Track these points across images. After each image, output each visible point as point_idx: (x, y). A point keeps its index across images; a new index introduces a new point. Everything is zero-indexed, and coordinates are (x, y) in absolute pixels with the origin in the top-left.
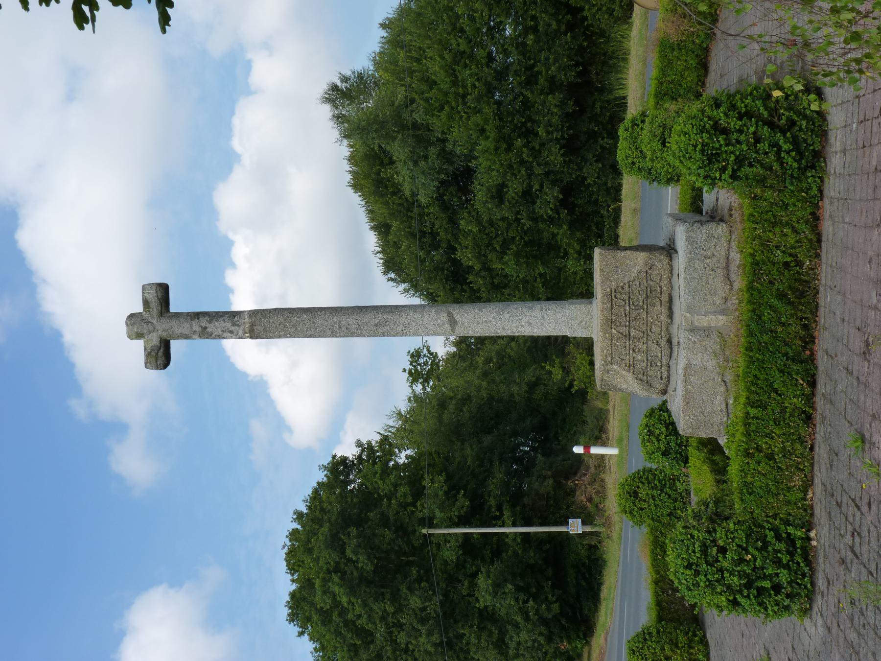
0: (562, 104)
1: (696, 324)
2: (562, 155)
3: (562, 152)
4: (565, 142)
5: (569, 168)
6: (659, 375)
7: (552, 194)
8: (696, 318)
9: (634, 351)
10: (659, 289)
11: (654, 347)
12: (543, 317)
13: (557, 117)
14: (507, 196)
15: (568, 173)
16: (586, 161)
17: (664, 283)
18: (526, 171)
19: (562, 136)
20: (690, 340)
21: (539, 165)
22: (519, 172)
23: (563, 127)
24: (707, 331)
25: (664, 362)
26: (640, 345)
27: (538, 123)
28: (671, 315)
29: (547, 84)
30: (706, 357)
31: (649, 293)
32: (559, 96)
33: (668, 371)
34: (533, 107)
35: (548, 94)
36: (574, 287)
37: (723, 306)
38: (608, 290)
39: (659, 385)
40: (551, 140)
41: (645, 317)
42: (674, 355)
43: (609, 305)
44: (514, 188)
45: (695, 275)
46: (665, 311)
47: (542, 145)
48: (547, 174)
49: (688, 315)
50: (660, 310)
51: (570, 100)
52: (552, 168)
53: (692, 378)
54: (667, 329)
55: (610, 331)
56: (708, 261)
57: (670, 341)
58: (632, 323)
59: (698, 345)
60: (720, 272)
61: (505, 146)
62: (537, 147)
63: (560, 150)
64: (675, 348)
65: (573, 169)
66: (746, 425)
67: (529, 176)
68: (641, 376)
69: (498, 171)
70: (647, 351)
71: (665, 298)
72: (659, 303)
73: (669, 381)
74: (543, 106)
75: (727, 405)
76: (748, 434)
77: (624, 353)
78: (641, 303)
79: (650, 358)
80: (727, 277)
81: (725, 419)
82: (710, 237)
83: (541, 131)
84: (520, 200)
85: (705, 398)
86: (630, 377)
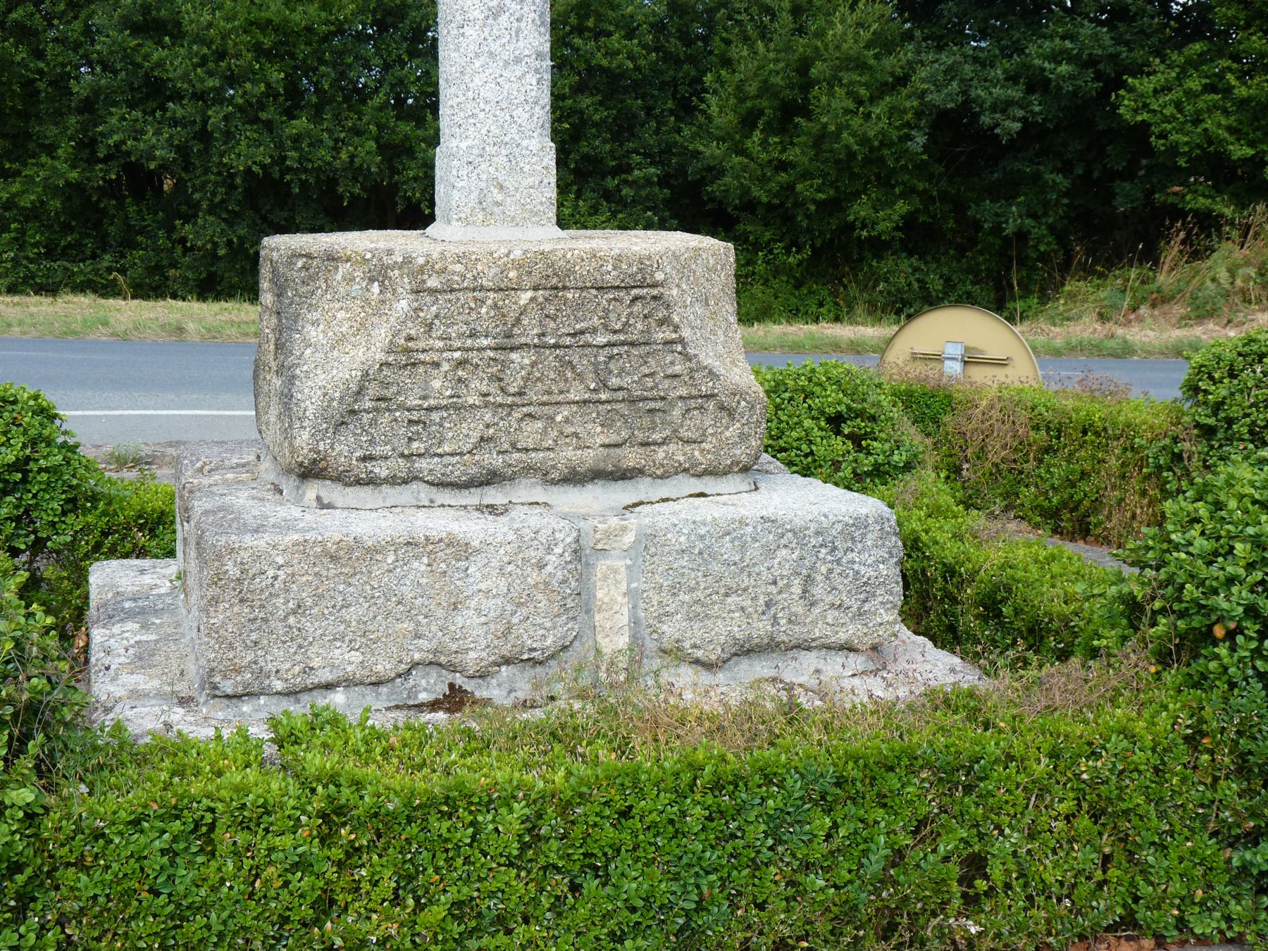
0: (355, 171)
1: (602, 566)
2: (248, 171)
3: (255, 168)
4: (276, 175)
5: (216, 184)
6: (378, 450)
7: (157, 143)
8: (621, 564)
9: (461, 363)
10: (657, 436)
11: (471, 430)
12: (518, 60)
13: (329, 159)
14: (149, 43)
15: (204, 185)
16: (230, 223)
17: (678, 453)
18: (213, 89)
19: (289, 169)
20: (549, 550)
21: (226, 118)
22: (210, 74)
23: (306, 170)
24: (579, 602)
25: (423, 464)
26: (479, 384)
27: (317, 117)
28: (574, 478)
29: (397, 139)
30: (492, 606)
31: (645, 405)
32: (375, 163)
33: (393, 481)
34: (350, 108)
35: (377, 140)
36: (603, 166)
37: (651, 645)
38: (659, 276)
39: (344, 450)
40: (280, 146)
41: (571, 396)
42: (446, 497)
43: (612, 278)
44: (174, 62)
45: (754, 551)
46: (589, 458)
47: (269, 125)
48: (204, 136)
49: (629, 538)
50: (594, 441)
51: (363, 188)
52: (219, 146)
53: (420, 566)
54: (529, 470)
55: (527, 282)
56: (797, 590)
57: (491, 478)
58: (550, 357)
59: (534, 577)
60: (761, 628)
61: (267, 42)
62: (264, 116)
63: (263, 166)
64: (472, 497)
65: (214, 194)
66: (448, 805)
67: (199, 96)
68: (373, 390)
69: (210, 25)
70: (458, 408)
71: (631, 457)
72: (614, 438)
73: (358, 482)
74: (351, 129)
75: (329, 686)
76: (416, 811)
77: (453, 331)
78: (614, 381)
79: (436, 416)
80: (746, 650)
81: (279, 685)
82: (866, 589)
83: (301, 123)
84: (141, 72)
85: (352, 614)
86: (370, 350)
